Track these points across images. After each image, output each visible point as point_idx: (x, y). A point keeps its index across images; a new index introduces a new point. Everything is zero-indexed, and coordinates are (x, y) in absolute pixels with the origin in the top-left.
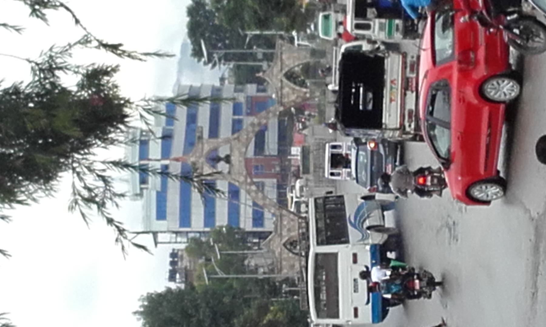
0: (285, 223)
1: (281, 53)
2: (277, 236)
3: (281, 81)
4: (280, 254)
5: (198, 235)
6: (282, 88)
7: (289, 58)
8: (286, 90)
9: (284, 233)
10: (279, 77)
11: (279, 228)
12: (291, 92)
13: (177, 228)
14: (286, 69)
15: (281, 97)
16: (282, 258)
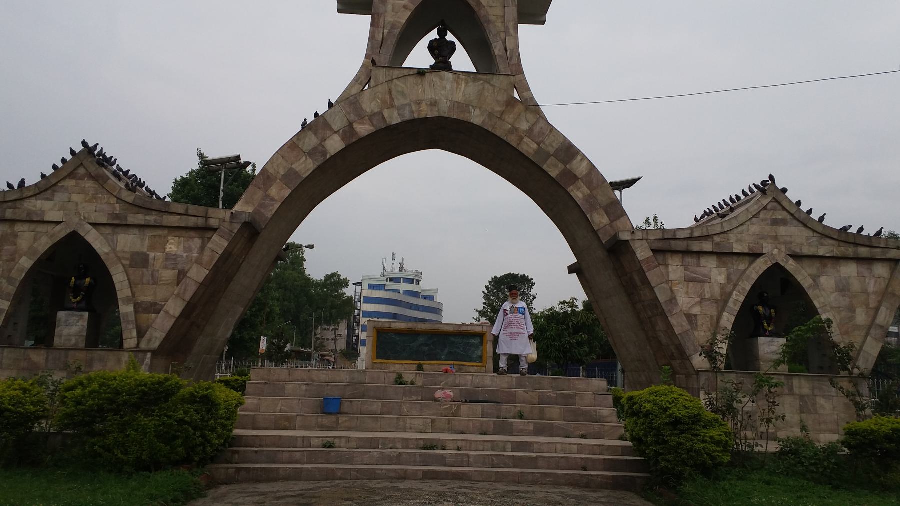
0: (173, 246)
1: (858, 259)
3: (755, 255)
4: (31, 220)
5: (359, 308)
6: (723, 255)
7: (843, 288)
9: (128, 241)
11: (152, 218)
12: (713, 289)
13: (364, 294)
15: (687, 252)
16: (19, 227)
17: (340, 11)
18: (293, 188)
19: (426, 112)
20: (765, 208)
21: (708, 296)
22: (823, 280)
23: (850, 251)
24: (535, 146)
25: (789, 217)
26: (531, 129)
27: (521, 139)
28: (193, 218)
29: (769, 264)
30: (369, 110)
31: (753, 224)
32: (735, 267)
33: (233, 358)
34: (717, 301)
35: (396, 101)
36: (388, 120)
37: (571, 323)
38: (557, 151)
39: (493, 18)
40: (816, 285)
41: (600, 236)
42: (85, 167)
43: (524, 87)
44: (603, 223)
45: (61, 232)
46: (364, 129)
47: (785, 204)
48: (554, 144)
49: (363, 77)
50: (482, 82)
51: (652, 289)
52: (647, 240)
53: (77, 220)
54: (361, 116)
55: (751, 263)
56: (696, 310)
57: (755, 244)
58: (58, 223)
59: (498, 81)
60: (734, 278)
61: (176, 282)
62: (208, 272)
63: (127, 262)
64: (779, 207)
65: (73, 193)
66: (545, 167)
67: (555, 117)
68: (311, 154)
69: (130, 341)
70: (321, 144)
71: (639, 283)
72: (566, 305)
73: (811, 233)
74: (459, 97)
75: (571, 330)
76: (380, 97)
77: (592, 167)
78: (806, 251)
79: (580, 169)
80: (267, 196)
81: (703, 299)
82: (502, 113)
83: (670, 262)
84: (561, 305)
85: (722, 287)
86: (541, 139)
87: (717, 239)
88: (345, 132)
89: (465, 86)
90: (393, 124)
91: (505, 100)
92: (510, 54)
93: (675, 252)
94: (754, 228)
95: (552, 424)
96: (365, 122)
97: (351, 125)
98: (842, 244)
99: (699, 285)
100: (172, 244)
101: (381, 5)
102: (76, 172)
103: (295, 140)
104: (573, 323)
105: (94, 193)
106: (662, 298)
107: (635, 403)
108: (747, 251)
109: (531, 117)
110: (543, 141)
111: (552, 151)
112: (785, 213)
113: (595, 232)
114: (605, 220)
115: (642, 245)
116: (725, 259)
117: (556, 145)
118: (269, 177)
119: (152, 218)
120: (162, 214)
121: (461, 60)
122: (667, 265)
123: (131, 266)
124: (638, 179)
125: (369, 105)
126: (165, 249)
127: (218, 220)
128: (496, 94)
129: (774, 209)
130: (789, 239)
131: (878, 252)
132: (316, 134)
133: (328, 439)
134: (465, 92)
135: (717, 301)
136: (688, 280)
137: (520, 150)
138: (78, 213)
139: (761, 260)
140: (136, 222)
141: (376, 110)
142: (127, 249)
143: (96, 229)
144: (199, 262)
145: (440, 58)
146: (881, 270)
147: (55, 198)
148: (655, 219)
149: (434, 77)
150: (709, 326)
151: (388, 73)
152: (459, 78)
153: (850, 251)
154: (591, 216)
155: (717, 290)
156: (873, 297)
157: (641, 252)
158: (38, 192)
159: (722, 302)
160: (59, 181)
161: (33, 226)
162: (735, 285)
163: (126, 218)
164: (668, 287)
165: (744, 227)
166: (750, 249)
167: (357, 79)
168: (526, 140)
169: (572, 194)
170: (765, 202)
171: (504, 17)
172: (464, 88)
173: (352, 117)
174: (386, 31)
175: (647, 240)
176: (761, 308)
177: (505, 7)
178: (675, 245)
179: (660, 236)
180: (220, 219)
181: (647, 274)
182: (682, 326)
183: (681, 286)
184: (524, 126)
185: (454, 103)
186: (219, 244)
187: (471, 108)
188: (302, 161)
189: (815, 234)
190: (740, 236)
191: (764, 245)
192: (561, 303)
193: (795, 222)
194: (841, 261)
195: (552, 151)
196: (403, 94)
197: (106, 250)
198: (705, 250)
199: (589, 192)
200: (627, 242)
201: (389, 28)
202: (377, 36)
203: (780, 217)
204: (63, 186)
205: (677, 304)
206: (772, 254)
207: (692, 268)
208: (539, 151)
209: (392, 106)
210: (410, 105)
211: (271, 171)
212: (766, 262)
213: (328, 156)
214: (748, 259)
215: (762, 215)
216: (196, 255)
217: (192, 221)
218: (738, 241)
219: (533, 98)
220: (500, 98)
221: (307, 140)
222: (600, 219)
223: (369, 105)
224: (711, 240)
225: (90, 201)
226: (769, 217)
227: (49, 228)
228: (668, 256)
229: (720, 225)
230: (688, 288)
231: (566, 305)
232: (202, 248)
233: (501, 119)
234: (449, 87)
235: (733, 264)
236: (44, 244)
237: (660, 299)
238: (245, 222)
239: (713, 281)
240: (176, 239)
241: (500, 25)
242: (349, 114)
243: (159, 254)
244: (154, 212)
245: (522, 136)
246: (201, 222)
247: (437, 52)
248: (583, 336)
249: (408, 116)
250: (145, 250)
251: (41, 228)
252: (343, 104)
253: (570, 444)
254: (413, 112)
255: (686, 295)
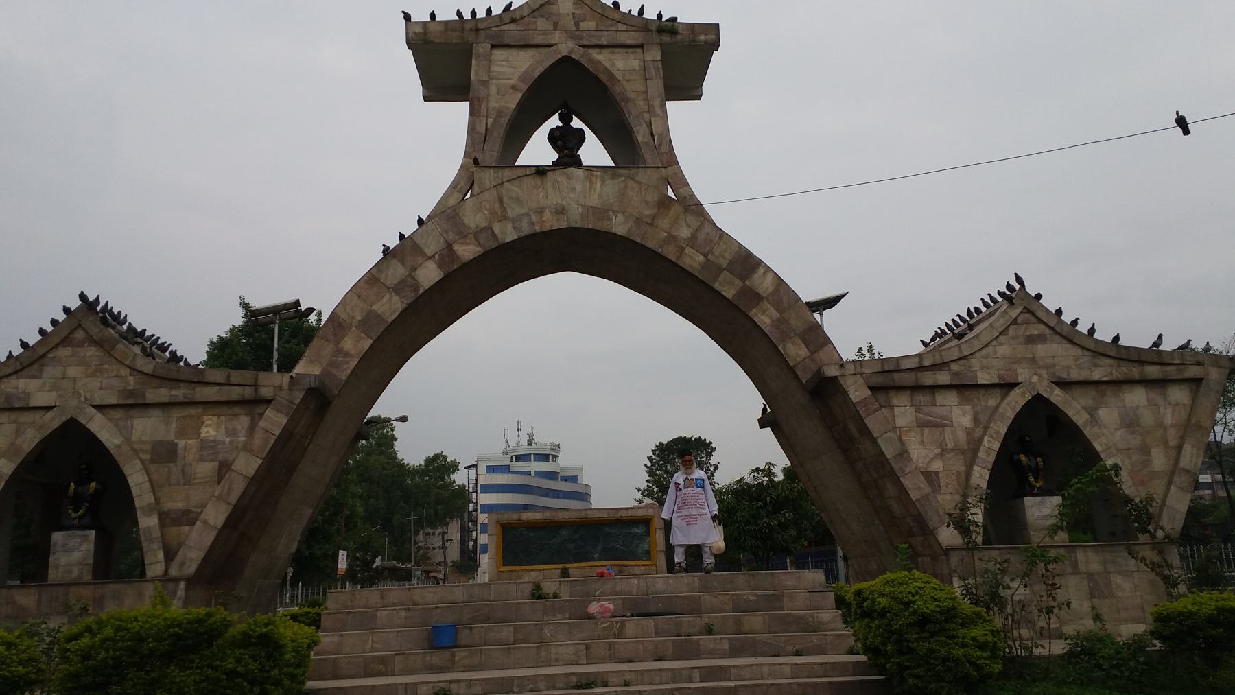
0: (211, 429)
1: (1147, 383)
2: (132, 382)
3: (1007, 386)
5: (475, 501)
6: (966, 389)
7: (1130, 422)
8: (960, 415)
9: (147, 427)
10: (1023, 374)
11: (179, 393)
12: (956, 436)
13: (480, 482)
14: (1078, 415)
15: (917, 388)
17: (426, 99)
18: (375, 338)
19: (551, 222)
20: (1015, 321)
21: (950, 445)
22: (1103, 413)
23: (1134, 371)
24: (701, 258)
25: (1047, 331)
26: (694, 237)
27: (682, 250)
28: (236, 388)
29: (1028, 397)
30: (473, 226)
31: (1001, 344)
32: (983, 404)
33: (300, 584)
34: (963, 452)
35: (509, 210)
36: (499, 237)
37: (768, 499)
38: (731, 262)
39: (632, 95)
40: (1094, 420)
41: (799, 373)
42: (84, 330)
43: (680, 182)
44: (801, 355)
45: (53, 421)
46: (467, 251)
47: (1041, 314)
48: (726, 255)
49: (462, 183)
50: (623, 178)
51: (874, 441)
52: (861, 374)
53: (74, 402)
54: (463, 234)
55: (1003, 398)
56: (937, 466)
57: (1006, 370)
58: (48, 409)
59: (644, 176)
60: (983, 418)
61: (216, 479)
62: (260, 461)
63: (147, 457)
64: (1034, 320)
65: (68, 366)
66: (716, 286)
67: (725, 218)
68: (398, 289)
69: (155, 567)
70: (410, 275)
71: (856, 434)
72: (760, 473)
73: (1079, 352)
74: (594, 200)
75: (770, 509)
76: (487, 206)
77: (780, 282)
78: (1075, 375)
79: (764, 285)
80: (339, 351)
81: (944, 450)
82: (654, 217)
83: (895, 401)
84: (753, 475)
85: (969, 432)
86: (708, 248)
87: (954, 367)
88: (442, 256)
89: (602, 185)
90: (507, 240)
91: (656, 199)
92: (658, 140)
93: (901, 388)
94: (1003, 350)
95: (754, 639)
96: (469, 241)
97: (449, 246)
98: (1122, 363)
99: (937, 431)
100: (208, 426)
101: (481, 87)
102: (73, 336)
103: (374, 272)
104: (772, 498)
105: (98, 363)
106: (889, 452)
107: (865, 599)
108: (995, 380)
109: (693, 221)
110: (711, 252)
111: (724, 263)
112: (1042, 326)
113: (791, 370)
114: (803, 352)
115: (856, 382)
116: (967, 393)
117: (729, 256)
118: (340, 325)
119: (179, 393)
120: (194, 385)
121: (593, 152)
122: (892, 407)
123: (153, 461)
124: (843, 296)
125: (473, 218)
126: (199, 434)
127: (271, 389)
128: (644, 193)
129: (1027, 322)
130: (1049, 361)
131: (1171, 371)
132: (402, 262)
133: (442, 685)
134: (601, 193)
135: (963, 452)
136: (922, 425)
137: (682, 265)
138: (76, 393)
139: (1016, 392)
140: (158, 400)
141: (483, 225)
142: (144, 439)
143: (103, 414)
144: (247, 448)
145: (565, 151)
146: (1179, 395)
147: (44, 375)
148: (870, 348)
149: (558, 177)
150: (957, 486)
151: (496, 175)
152: (592, 175)
153: (1134, 371)
154: (784, 346)
155: (962, 436)
156: (1172, 432)
157: (856, 391)
158: (21, 367)
159: (971, 453)
160: (49, 351)
161: (14, 416)
162: (986, 428)
163: (144, 396)
164: (896, 437)
165: (989, 350)
166: (1000, 377)
167: (454, 185)
168: (688, 251)
169: (756, 319)
170: (1014, 313)
171: (646, 92)
172: (601, 188)
173: (451, 236)
174: (490, 120)
175: (861, 374)
176: (1023, 458)
177: (647, 80)
178: (899, 379)
179: (878, 368)
180: (274, 387)
181: (866, 421)
182: (919, 488)
183: (913, 434)
184: (684, 233)
185: (588, 209)
186: (274, 421)
187: (611, 213)
188: (385, 300)
189: (1086, 353)
190: (985, 361)
191: (1019, 371)
192: (753, 471)
193: (1057, 338)
194: (1124, 386)
195: (724, 263)
196: (518, 200)
197: (117, 442)
198: (940, 383)
199: (779, 315)
200: (834, 379)
201: (494, 116)
202: (478, 128)
203: (1036, 333)
204: (54, 357)
205: (910, 459)
206: (1031, 383)
207: (926, 409)
208: (707, 265)
209: (504, 218)
210: (528, 215)
211: (343, 316)
212: (1024, 393)
213: (421, 291)
214: (998, 391)
215: (1011, 332)
216: (244, 439)
217: (236, 393)
218: (982, 368)
219: (693, 196)
220: (649, 198)
221: (391, 271)
222: (796, 351)
223: (473, 218)
224: (947, 369)
225: (93, 375)
226: (1021, 333)
227: (37, 417)
228: (892, 394)
229: (957, 349)
230: (922, 435)
231: (760, 473)
232: (252, 429)
233: (653, 226)
234: (579, 188)
235: (980, 400)
236: (30, 439)
237: (886, 453)
238: (310, 388)
239: (955, 424)
240: (215, 419)
241: (641, 103)
242: (446, 232)
243: (190, 442)
244: (182, 384)
245: (682, 247)
246: (248, 392)
247: (560, 143)
248: (787, 514)
249: (526, 230)
250: (172, 437)
251: (26, 417)
252: (437, 219)
253: (781, 665)
254: (533, 224)
255: (921, 447)
